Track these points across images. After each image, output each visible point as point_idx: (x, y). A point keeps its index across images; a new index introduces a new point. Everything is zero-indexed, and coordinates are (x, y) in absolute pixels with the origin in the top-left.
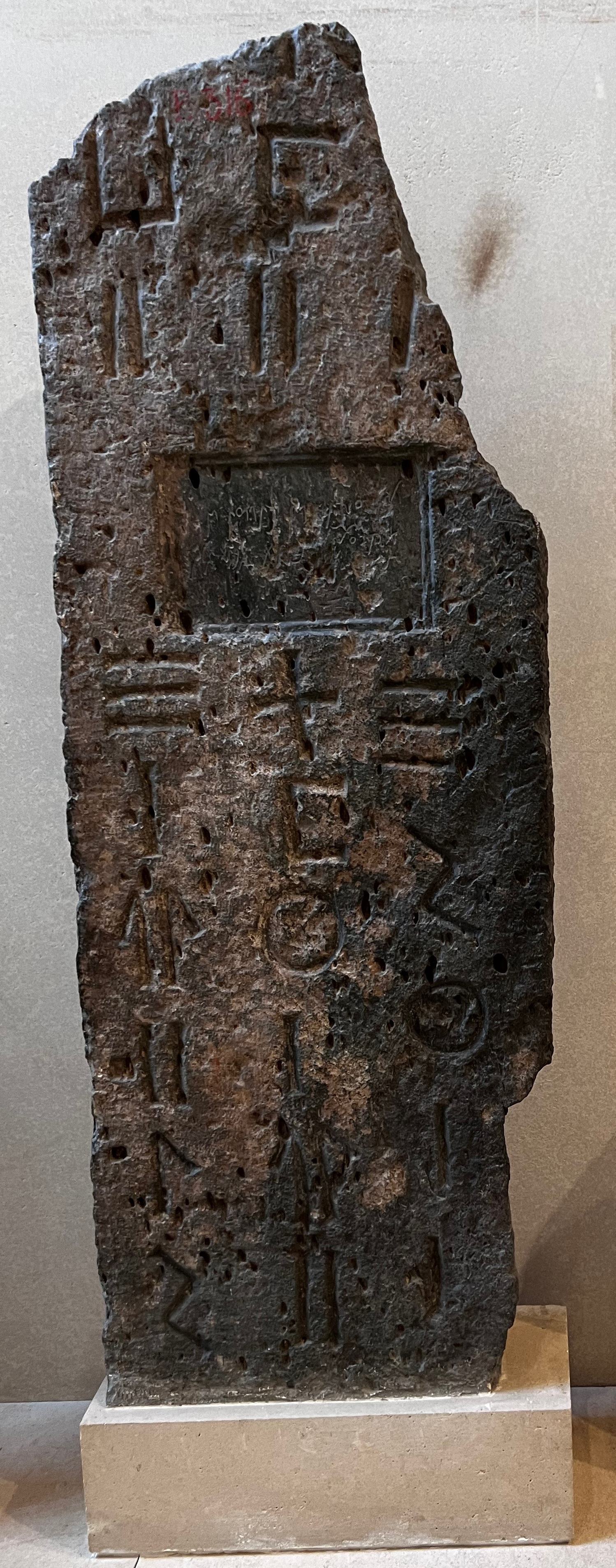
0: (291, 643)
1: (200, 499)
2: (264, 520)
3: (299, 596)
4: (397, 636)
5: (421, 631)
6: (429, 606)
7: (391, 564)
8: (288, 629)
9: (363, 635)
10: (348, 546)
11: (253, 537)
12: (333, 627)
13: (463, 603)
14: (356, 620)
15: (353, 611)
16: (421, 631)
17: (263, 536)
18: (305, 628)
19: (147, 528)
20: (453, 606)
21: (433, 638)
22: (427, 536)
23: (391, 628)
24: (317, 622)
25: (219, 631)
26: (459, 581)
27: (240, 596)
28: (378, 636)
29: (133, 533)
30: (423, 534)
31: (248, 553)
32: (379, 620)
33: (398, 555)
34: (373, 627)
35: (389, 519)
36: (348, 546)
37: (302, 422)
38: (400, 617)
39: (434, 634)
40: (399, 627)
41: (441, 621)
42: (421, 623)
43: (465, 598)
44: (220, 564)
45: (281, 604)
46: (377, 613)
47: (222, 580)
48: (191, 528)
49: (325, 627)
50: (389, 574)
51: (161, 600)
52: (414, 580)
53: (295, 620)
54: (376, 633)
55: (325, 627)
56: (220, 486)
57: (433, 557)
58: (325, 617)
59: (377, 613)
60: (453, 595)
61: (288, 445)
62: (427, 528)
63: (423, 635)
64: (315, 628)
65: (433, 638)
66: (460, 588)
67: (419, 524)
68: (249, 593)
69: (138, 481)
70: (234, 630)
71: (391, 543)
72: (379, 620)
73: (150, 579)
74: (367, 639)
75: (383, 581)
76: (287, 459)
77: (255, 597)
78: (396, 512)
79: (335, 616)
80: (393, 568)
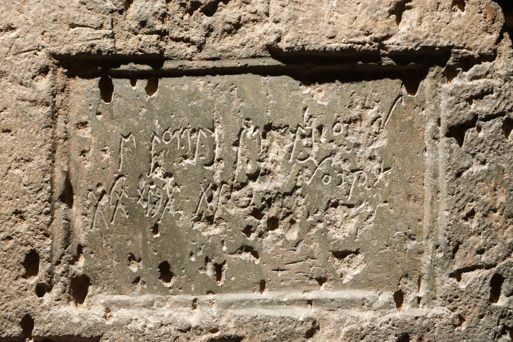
0: (231, 325)
1: (112, 118)
2: (201, 149)
3: (246, 256)
4: (385, 319)
5: (421, 311)
6: (433, 276)
7: (379, 213)
8: (228, 305)
9: (335, 316)
10: (319, 187)
11: (185, 172)
12: (291, 303)
13: (485, 272)
14: (324, 292)
15: (321, 281)
16: (421, 311)
17: (199, 171)
18: (251, 303)
19: (37, 158)
20: (469, 276)
21: (438, 323)
22: (435, 176)
23: (375, 306)
24: (267, 295)
25: (126, 305)
26: (480, 241)
27: (160, 255)
28: (357, 319)
29: (14, 165)
30: (428, 174)
31: (176, 195)
32: (359, 294)
33: (391, 201)
34: (350, 303)
35: (381, 150)
36: (319, 187)
37: (267, 14)
38: (388, 289)
39: (440, 317)
40: (387, 306)
41: (451, 299)
42: (419, 299)
43: (488, 267)
44: (133, 211)
45: (218, 269)
46: (355, 283)
47: (135, 234)
48: (97, 159)
49: (280, 303)
50: (376, 228)
51: (49, 260)
52: (411, 237)
53: (237, 291)
54: (355, 312)
55: (280, 303)
56: (142, 100)
57: (444, 206)
58: (280, 288)
59: (355, 283)
60: (470, 261)
61: (243, 45)
62: (436, 165)
63: (424, 318)
64: (266, 304)
65: (438, 323)
66: (481, 252)
67: (423, 159)
68: (174, 251)
69: (27, 92)
70: (149, 305)
71: (381, 184)
72: (359, 294)
73: (34, 231)
74: (341, 322)
75: (366, 238)
76: (242, 63)
77: (182, 258)
78: (392, 141)
79: (294, 286)
80: (383, 220)
